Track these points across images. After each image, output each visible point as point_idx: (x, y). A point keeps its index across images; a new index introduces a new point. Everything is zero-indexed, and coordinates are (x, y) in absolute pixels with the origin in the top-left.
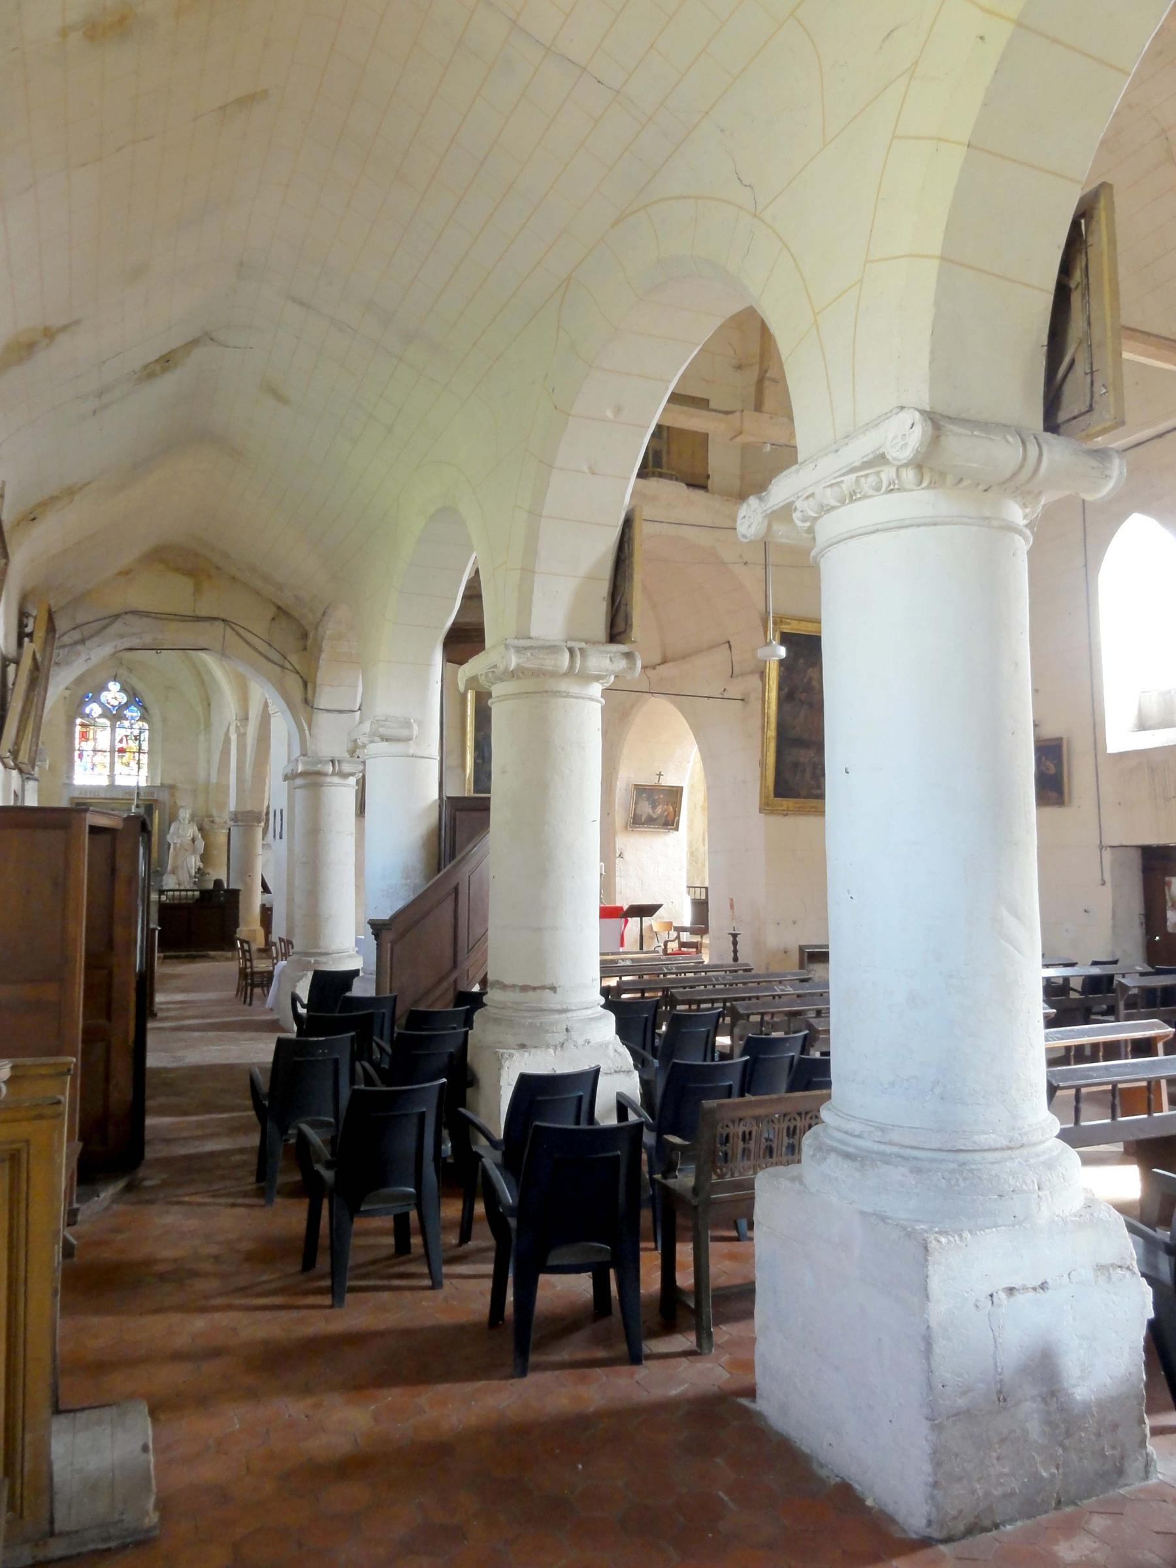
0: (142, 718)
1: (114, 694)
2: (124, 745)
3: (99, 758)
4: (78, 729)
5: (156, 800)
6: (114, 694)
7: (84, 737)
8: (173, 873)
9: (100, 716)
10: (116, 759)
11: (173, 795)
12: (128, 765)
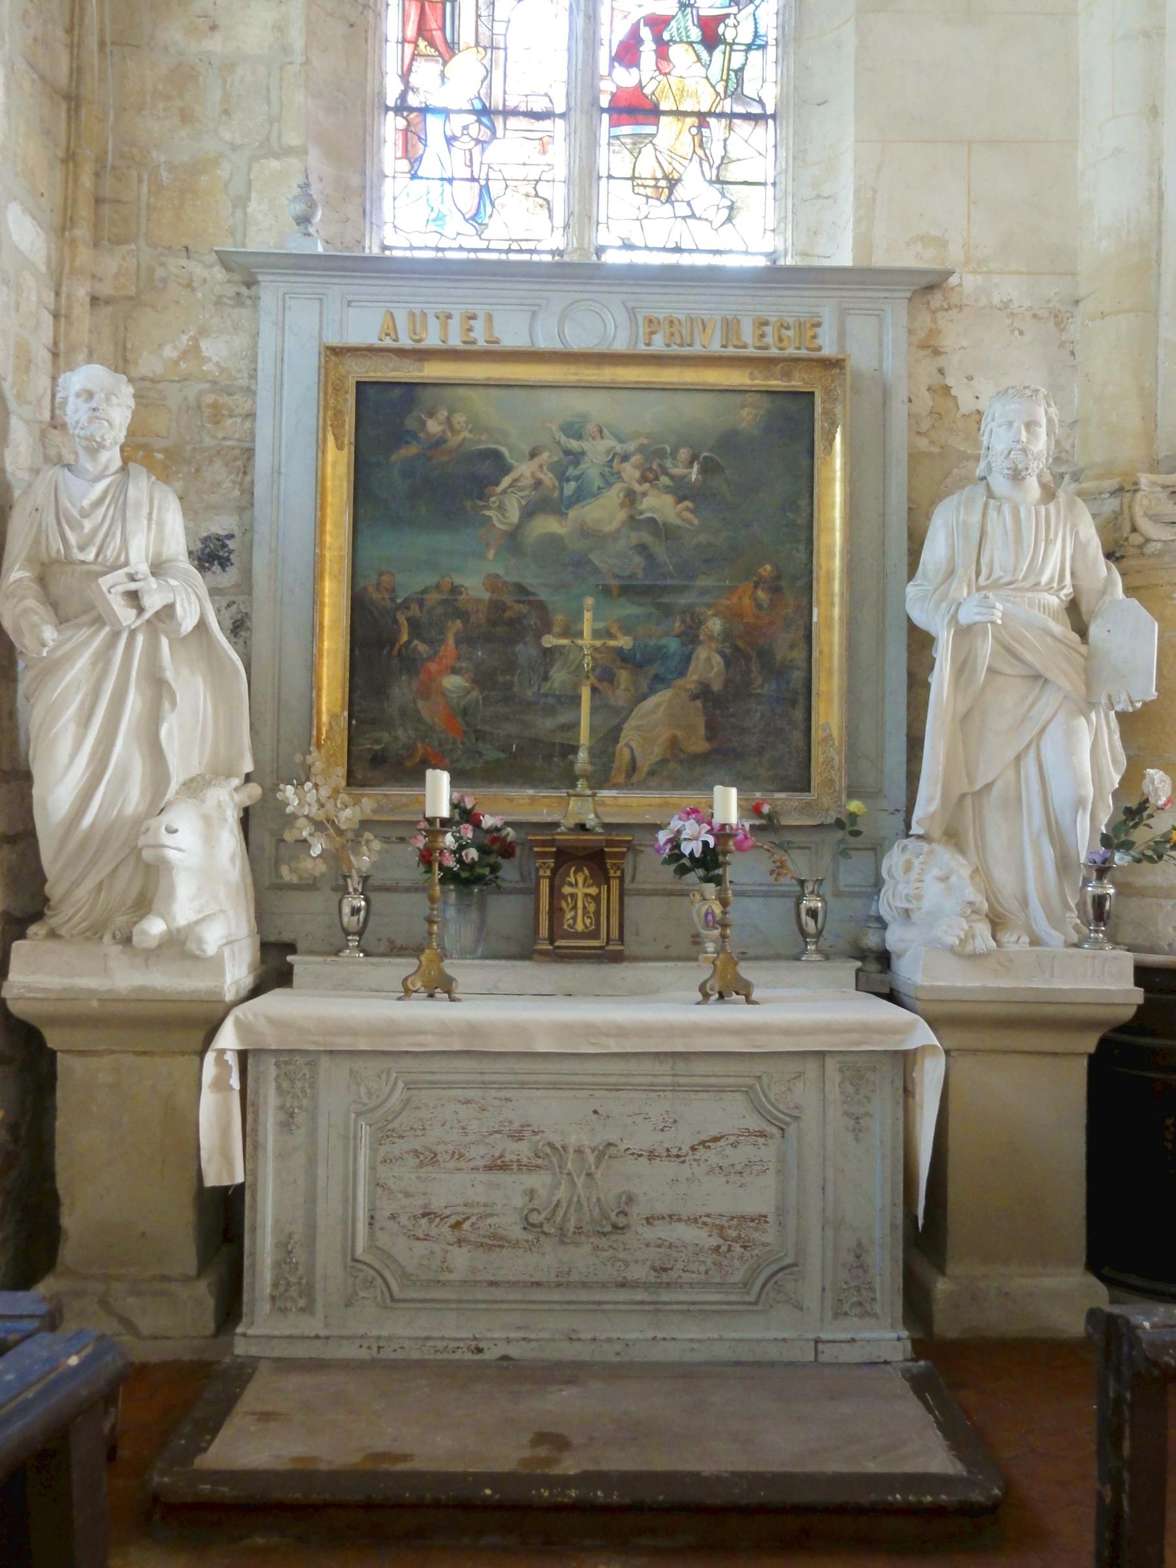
2: (644, 74)
3: (512, 148)
5: (834, 365)
8: (953, 837)
10: (613, 159)
11: (930, 347)
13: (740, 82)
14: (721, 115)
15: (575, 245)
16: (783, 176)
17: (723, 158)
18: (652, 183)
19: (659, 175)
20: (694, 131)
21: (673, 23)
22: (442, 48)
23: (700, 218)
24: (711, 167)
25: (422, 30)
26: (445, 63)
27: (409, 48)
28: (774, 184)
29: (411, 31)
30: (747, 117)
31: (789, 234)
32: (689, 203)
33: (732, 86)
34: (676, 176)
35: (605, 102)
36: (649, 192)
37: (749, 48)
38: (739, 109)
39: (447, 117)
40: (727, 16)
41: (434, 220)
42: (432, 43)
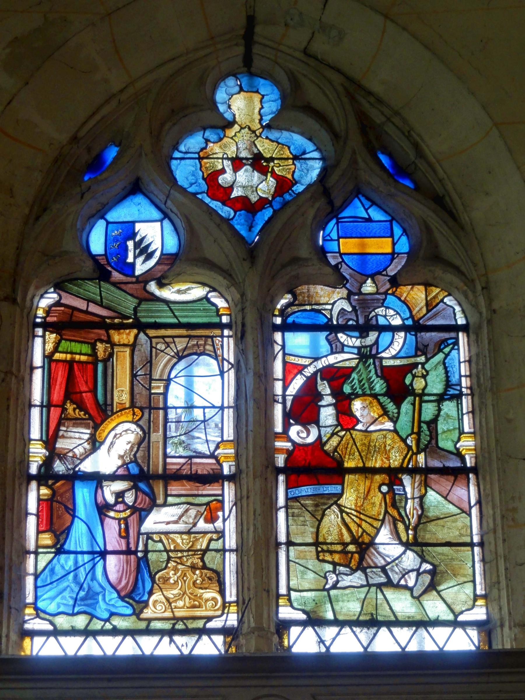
0: (426, 262)
1: (246, 138)
4: (39, 349)
6: (246, 138)
7: (83, 399)
9: (171, 268)
12: (358, 553)
13: (434, 434)
14: (413, 471)
15: (253, 625)
16: (491, 535)
17: (420, 517)
18: (339, 548)
19: (347, 538)
20: (385, 489)
21: (354, 375)
22: (93, 412)
23: (398, 586)
24: (407, 529)
25: (71, 393)
26: (96, 427)
27: (55, 413)
28: (481, 544)
29: (57, 395)
30: (444, 471)
31: (504, 601)
32: (383, 569)
33: (425, 439)
34: (367, 539)
35: (280, 460)
36: (337, 558)
37: (441, 398)
38: (436, 463)
39: (99, 486)
40: (415, 365)
41: (82, 599)
42: (81, 406)
